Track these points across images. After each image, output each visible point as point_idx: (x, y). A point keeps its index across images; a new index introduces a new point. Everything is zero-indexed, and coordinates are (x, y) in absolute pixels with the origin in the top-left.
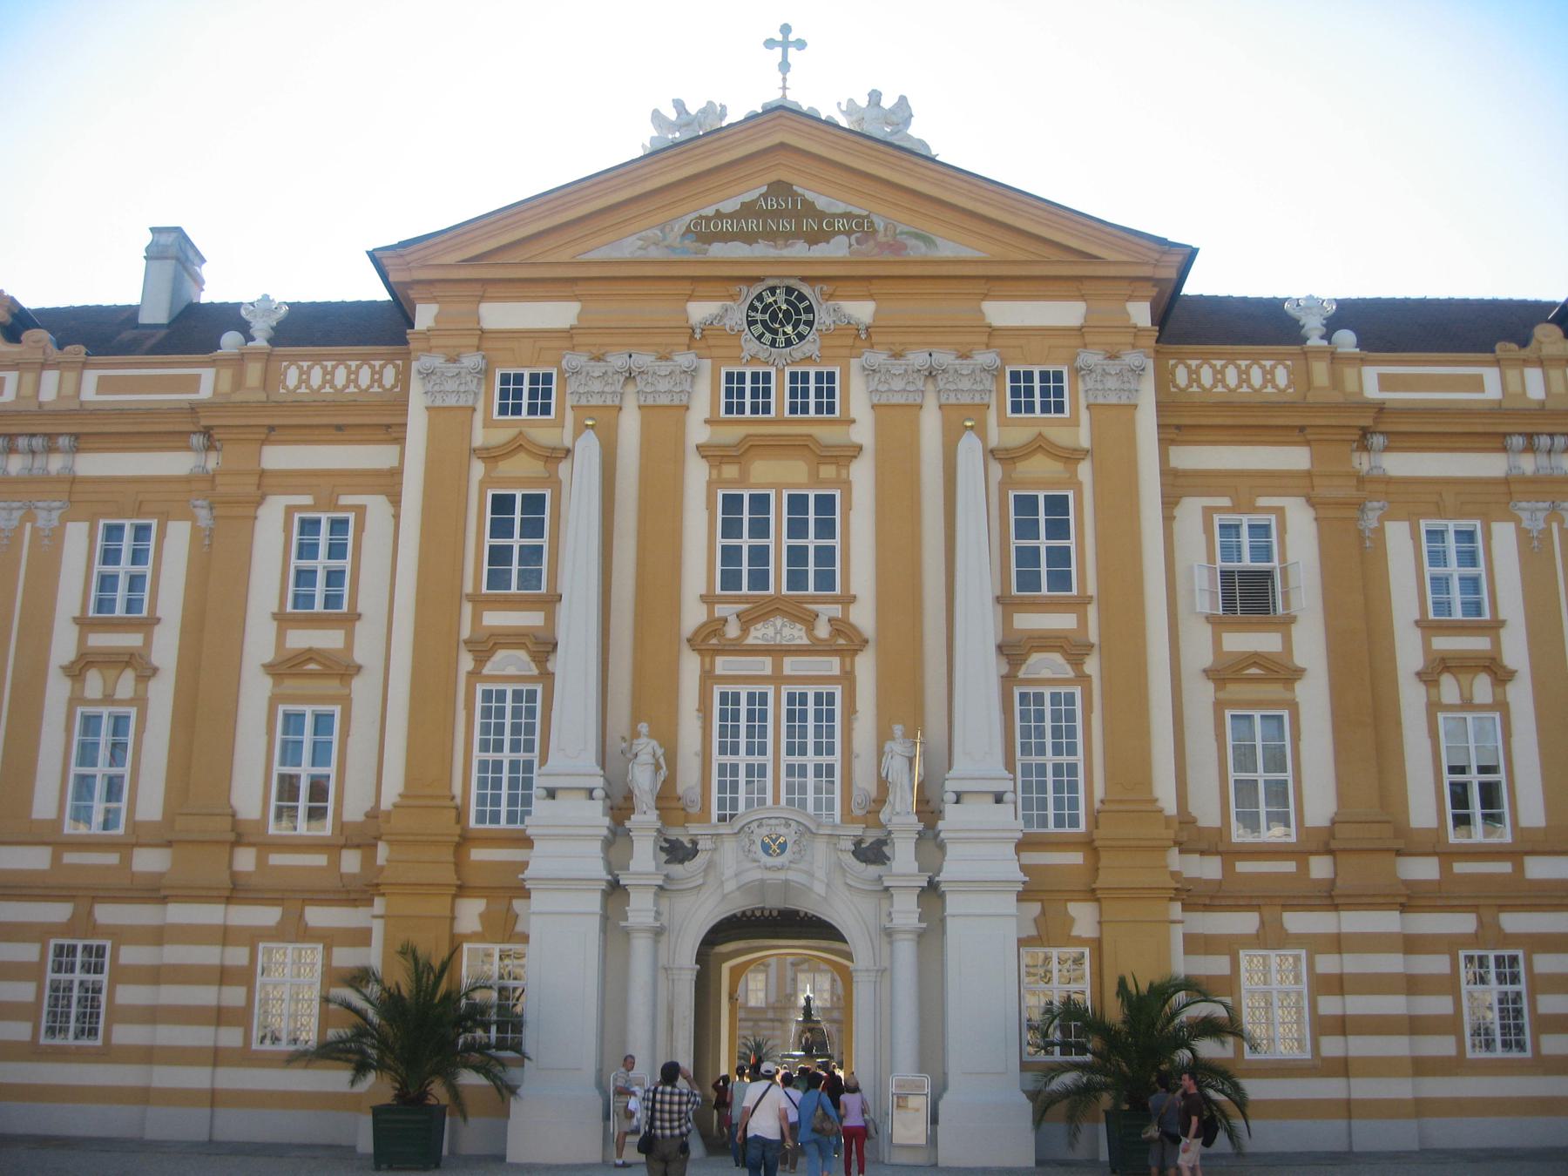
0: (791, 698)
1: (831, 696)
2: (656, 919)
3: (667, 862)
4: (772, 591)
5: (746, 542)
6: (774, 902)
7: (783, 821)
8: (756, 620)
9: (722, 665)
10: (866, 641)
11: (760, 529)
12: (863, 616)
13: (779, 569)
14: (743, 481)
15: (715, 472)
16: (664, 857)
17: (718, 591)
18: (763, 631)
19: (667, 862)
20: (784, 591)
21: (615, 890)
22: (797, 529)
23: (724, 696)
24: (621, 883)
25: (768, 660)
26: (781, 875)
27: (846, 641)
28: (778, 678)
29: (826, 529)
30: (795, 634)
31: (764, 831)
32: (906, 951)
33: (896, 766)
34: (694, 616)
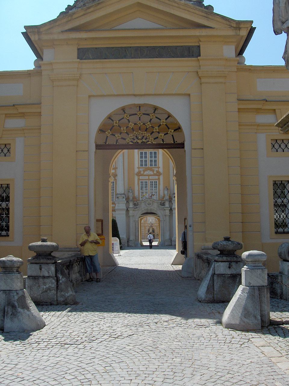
1: (157, 182)
4: (148, 166)
5: (144, 159)
8: (145, 171)
9: (141, 177)
10: (161, 174)
11: (146, 157)
12: (161, 170)
13: (149, 163)
17: (140, 167)
21: (127, 210)
22: (151, 157)
23: (141, 182)
26: (150, 208)
27: (158, 174)
28: (149, 179)
29: (155, 157)
30: (151, 173)
31: (148, 202)
32: (168, 218)
33: (166, 192)
34: (136, 170)
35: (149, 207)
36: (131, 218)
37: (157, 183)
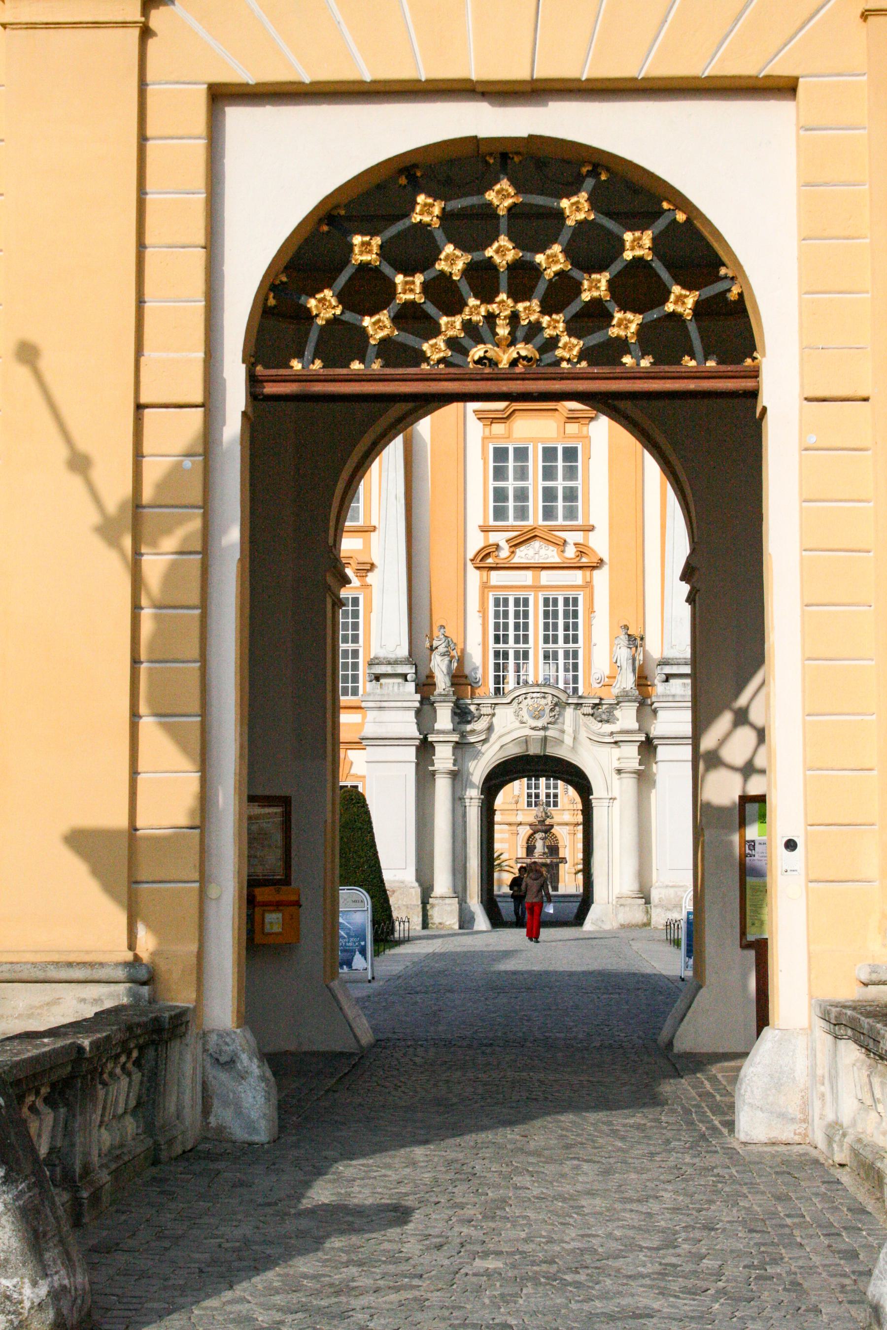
0: (546, 601)
1: (575, 600)
2: (454, 765)
3: (459, 723)
6: (534, 750)
7: (543, 695)
9: (496, 577)
11: (522, 474)
13: (536, 504)
14: (508, 437)
15: (487, 430)
16: (457, 719)
17: (491, 522)
18: (525, 552)
19: (459, 723)
20: (541, 522)
22: (549, 473)
24: (430, 739)
25: (529, 574)
28: (536, 587)
29: (571, 473)
33: (624, 654)
34: (475, 542)
35: (533, 729)
36: (442, 787)
37: (580, 608)
